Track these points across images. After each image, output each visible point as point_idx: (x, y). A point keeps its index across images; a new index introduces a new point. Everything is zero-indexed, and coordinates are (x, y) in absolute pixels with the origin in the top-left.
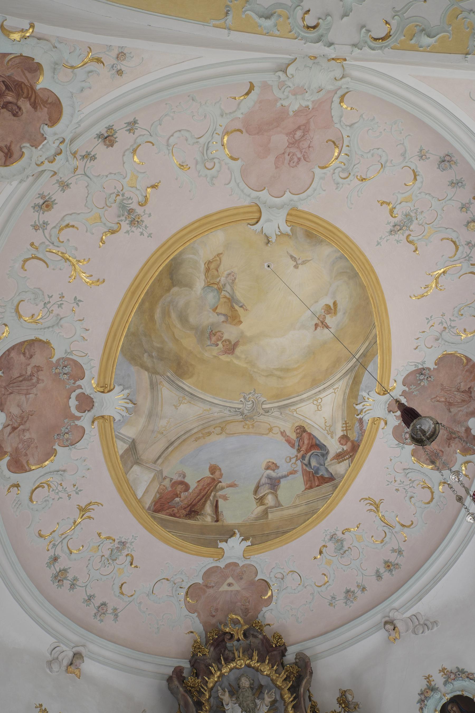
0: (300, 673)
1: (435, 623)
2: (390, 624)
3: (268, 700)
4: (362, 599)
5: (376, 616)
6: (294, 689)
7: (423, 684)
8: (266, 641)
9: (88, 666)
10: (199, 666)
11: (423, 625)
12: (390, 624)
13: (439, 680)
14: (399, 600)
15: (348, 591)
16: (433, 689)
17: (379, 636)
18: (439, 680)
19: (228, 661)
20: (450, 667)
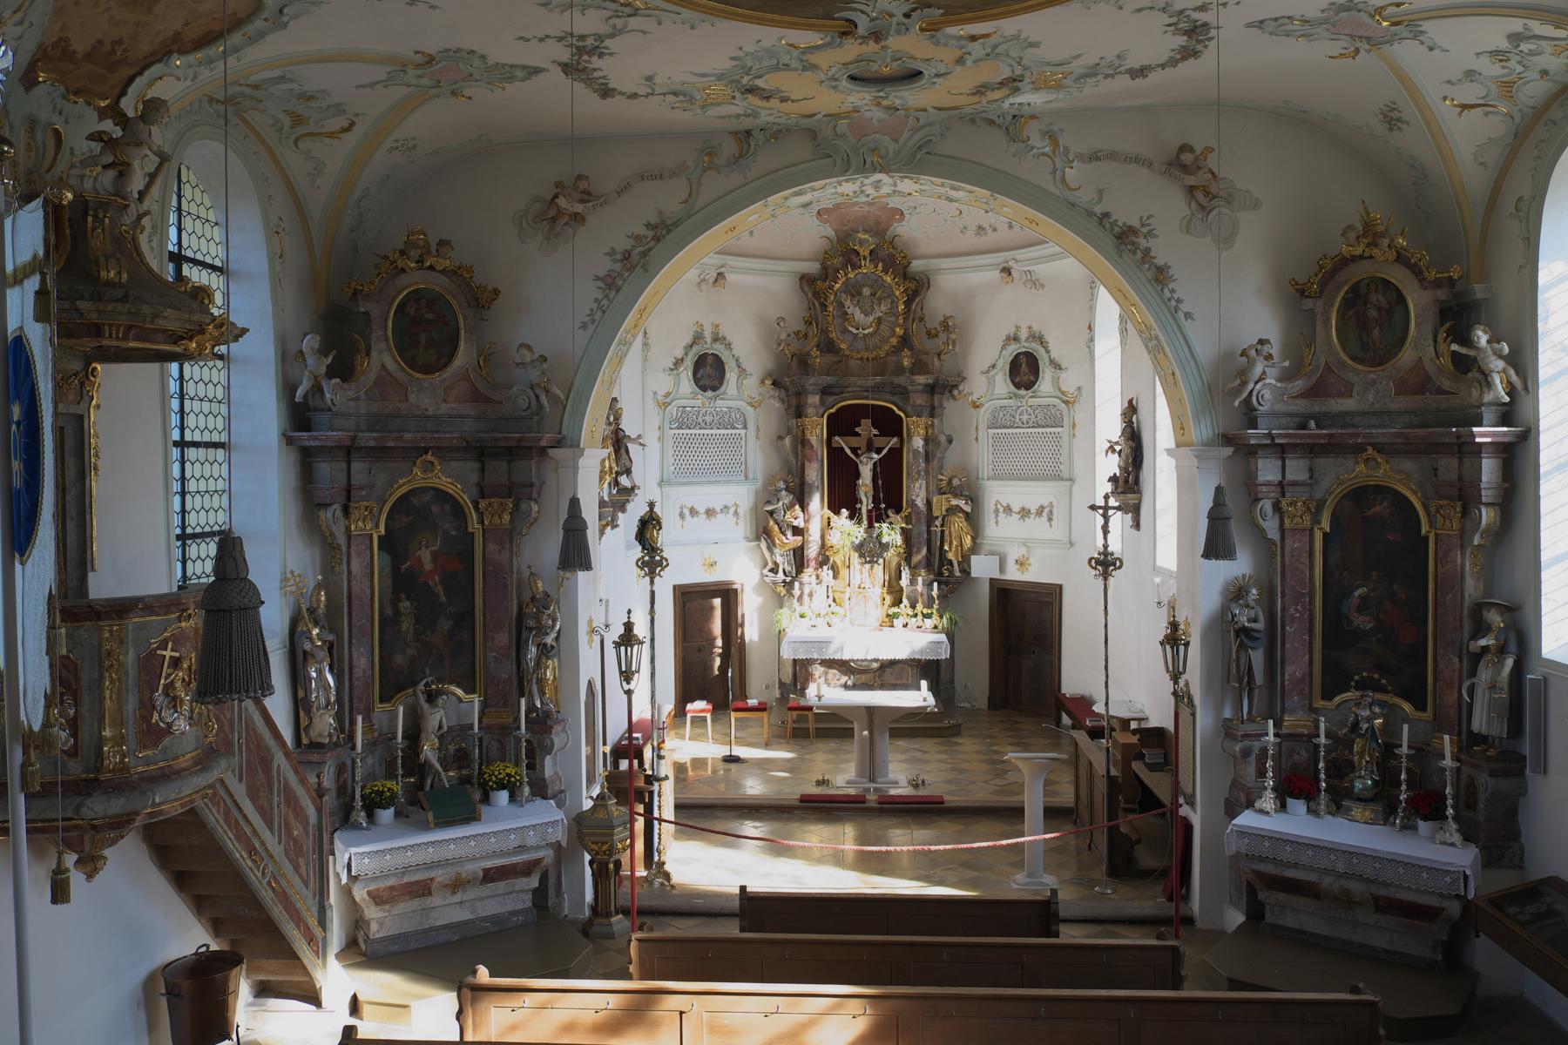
0: (917, 286)
1: (1042, 286)
2: (1007, 271)
3: (883, 308)
4: (990, 239)
5: (999, 258)
6: (908, 304)
7: (1012, 331)
8: (892, 258)
9: (731, 277)
10: (827, 274)
11: (1035, 283)
12: (1007, 271)
13: (1024, 334)
14: (1021, 254)
15: (980, 228)
16: (1016, 339)
17: (995, 274)
18: (1024, 334)
19: (854, 267)
20: (1036, 328)
